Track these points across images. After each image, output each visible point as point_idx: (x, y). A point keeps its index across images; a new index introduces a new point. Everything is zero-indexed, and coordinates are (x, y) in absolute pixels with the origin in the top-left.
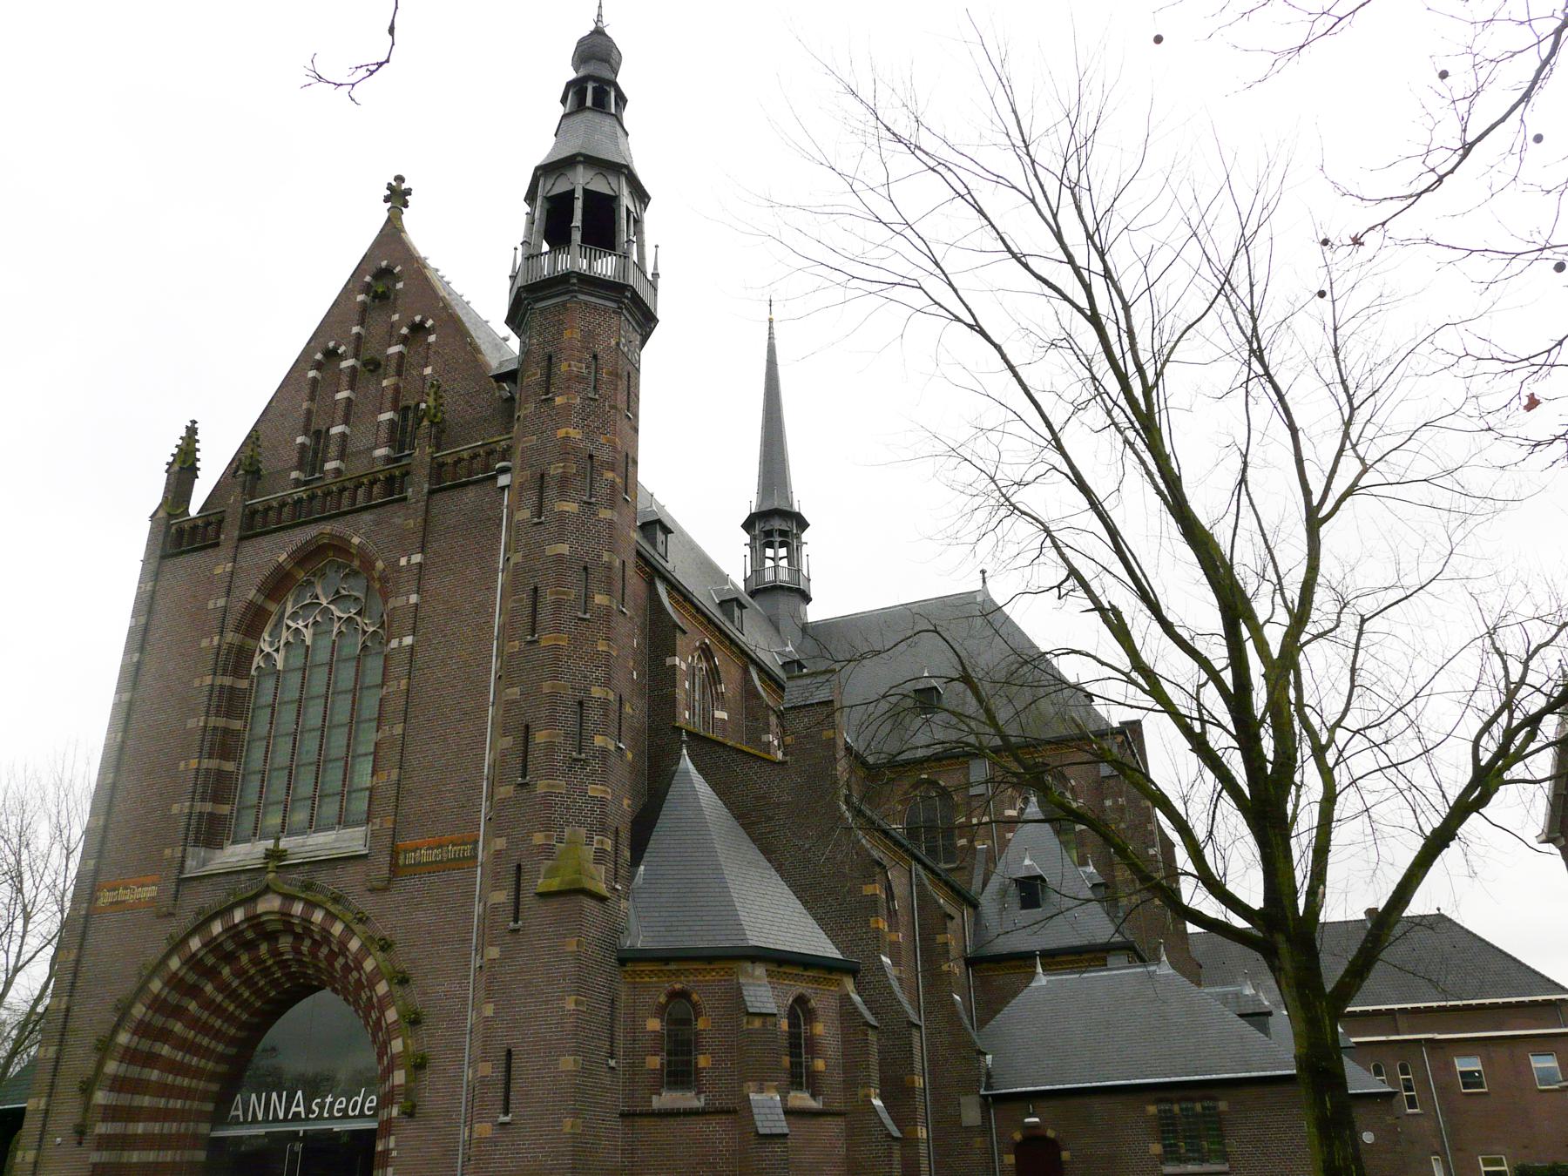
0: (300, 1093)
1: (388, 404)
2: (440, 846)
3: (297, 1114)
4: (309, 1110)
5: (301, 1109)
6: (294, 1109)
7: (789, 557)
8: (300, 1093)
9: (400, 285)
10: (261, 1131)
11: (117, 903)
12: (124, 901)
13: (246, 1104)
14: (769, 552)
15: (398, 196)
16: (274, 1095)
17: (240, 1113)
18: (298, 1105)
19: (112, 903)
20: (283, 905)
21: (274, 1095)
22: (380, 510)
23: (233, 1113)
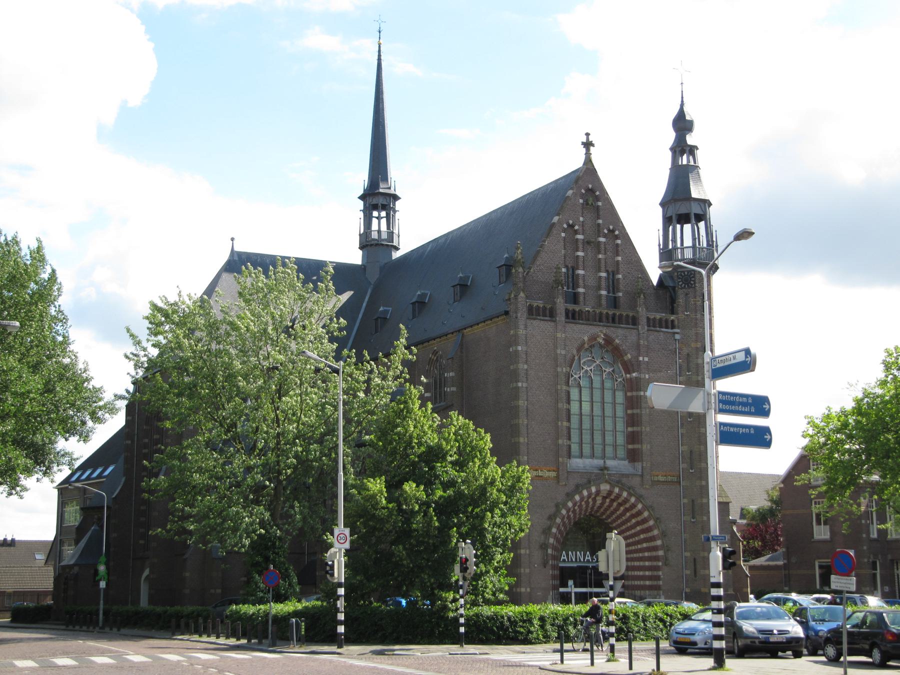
0: (588, 553)
1: (603, 269)
2: (665, 476)
3: (588, 561)
4: (593, 559)
5: (590, 558)
6: (586, 558)
7: (388, 217)
8: (588, 553)
9: (600, 204)
10: (575, 565)
11: (539, 476)
12: (542, 476)
13: (567, 555)
14: (375, 214)
15: (588, 145)
16: (578, 553)
17: (566, 558)
18: (588, 557)
19: (536, 476)
20: (610, 488)
21: (578, 553)
22: (625, 330)
23: (562, 558)
